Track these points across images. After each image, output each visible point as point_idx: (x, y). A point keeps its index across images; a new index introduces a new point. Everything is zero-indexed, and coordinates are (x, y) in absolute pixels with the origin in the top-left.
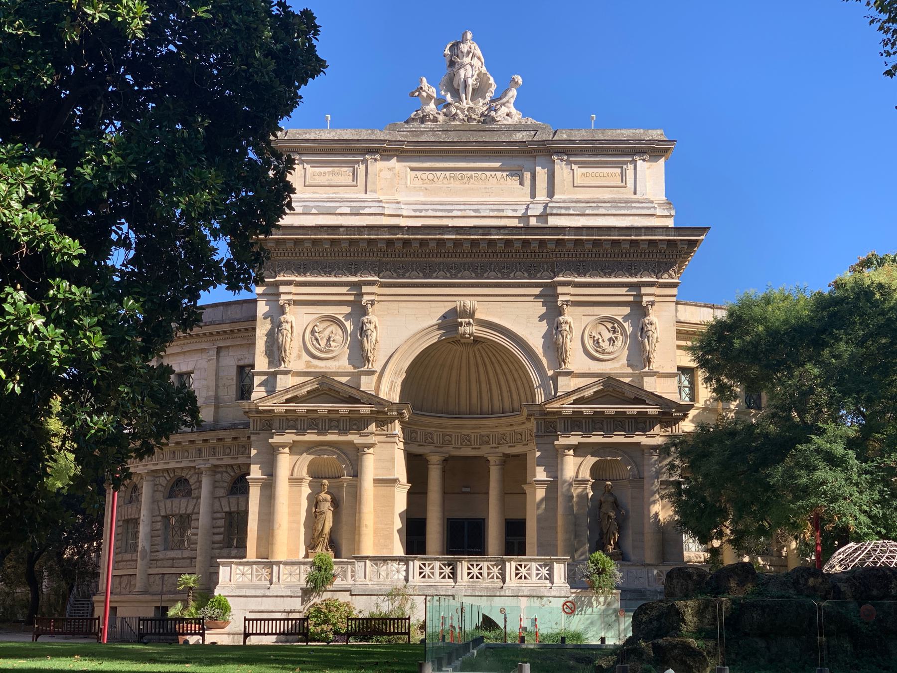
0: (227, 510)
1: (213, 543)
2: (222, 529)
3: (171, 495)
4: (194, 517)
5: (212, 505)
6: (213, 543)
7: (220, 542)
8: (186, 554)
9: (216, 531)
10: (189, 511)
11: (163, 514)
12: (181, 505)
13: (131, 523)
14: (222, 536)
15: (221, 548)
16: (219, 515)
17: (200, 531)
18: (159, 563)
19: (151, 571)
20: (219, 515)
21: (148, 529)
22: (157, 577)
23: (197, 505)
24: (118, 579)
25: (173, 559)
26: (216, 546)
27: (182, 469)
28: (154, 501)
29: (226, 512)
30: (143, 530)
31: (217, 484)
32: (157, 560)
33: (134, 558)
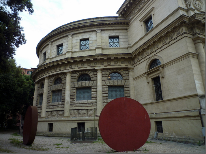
0: (109, 85)
1: (103, 97)
2: (107, 92)
3: (79, 80)
6: (103, 97)
7: (107, 97)
9: (104, 92)
14: (107, 94)
15: (107, 99)
16: (105, 87)
18: (75, 105)
19: (71, 108)
20: (105, 87)
22: (75, 111)
25: (83, 104)
27: (86, 70)
31: (103, 75)
32: (74, 104)
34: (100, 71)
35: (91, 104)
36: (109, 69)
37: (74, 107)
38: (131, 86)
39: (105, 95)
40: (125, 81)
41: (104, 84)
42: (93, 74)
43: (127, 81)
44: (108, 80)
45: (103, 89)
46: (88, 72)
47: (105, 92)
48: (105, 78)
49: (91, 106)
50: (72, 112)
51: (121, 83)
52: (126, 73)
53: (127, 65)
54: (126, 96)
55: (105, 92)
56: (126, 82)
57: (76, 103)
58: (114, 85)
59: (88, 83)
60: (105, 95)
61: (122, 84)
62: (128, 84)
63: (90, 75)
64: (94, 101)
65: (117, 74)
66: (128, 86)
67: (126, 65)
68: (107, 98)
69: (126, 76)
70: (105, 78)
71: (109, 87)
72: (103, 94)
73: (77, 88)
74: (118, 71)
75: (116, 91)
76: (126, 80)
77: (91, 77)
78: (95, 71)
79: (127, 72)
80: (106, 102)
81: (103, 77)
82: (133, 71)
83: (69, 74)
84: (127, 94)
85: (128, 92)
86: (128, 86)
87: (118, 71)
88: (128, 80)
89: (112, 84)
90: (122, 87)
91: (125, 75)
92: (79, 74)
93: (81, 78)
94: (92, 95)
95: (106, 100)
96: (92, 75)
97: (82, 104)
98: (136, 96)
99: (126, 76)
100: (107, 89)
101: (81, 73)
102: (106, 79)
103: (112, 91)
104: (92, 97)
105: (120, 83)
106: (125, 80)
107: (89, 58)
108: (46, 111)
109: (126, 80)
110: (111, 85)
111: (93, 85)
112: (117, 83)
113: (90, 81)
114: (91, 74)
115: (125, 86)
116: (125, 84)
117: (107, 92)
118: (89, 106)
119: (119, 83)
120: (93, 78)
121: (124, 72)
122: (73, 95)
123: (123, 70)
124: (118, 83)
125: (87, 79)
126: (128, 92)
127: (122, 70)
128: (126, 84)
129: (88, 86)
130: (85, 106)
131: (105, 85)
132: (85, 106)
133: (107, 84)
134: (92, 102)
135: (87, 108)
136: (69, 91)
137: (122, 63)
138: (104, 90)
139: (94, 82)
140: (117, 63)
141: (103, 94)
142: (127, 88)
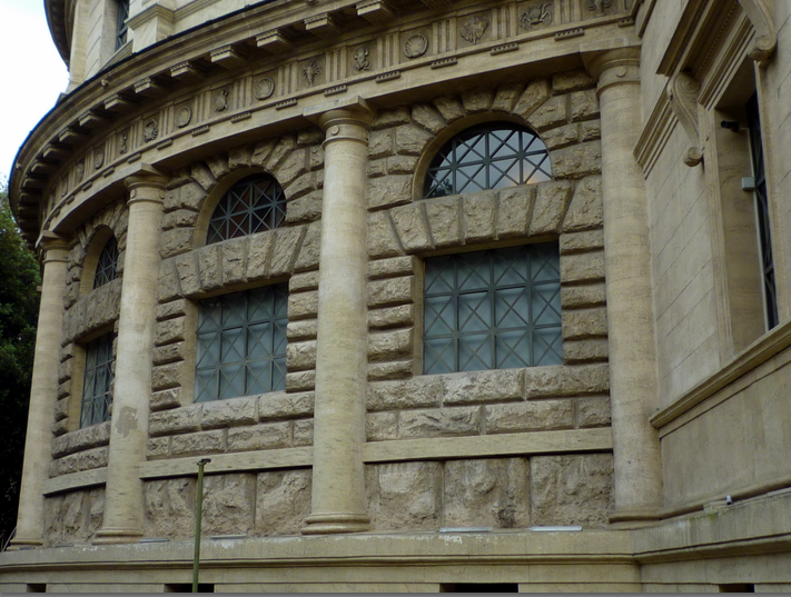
0: (421, 241)
2: (404, 312)
3: (216, 233)
4: (296, 281)
5: (363, 233)
7: (401, 354)
8: (274, 401)
9: (378, 317)
10: (278, 267)
11: (190, 287)
12: (252, 255)
13: (97, 341)
14: (404, 333)
15: (404, 374)
16: (388, 265)
17: (324, 325)
18: (177, 443)
20: (388, 265)
21: (145, 338)
22: (175, 486)
23: (310, 243)
24: (56, 503)
25: (225, 425)
26: (385, 367)
28: (166, 255)
29: (413, 252)
30: (131, 344)
31: (380, 165)
32: (171, 433)
33: (102, 437)
34: (346, 130)
35: (282, 426)
36: (426, 98)
37: (175, 455)
38: (616, 232)
39: (387, 341)
40: (571, 194)
41: (382, 235)
42: (300, 166)
43: (581, 186)
44: (417, 203)
45: (375, 286)
46: (268, 157)
47: (390, 314)
48: (393, 188)
49: (281, 445)
50: (155, 494)
51: (529, 215)
52: (577, 110)
53: (577, 33)
54: (576, 330)
55: (390, 314)
56: (577, 200)
57: (184, 421)
58: (471, 241)
59: (267, 243)
60: (387, 341)
61: (536, 226)
62: (591, 220)
63: (283, 176)
64: (297, 402)
65: (503, 134)
66: (587, 239)
67: (561, 37)
68: (404, 363)
69: (573, 142)
70: (393, 188)
71: (434, 260)
72: (373, 328)
73: (192, 299)
74: (504, 102)
75: (494, 297)
76: (573, 178)
77: (288, 192)
78: (310, 131)
79: (581, 102)
80: (390, 399)
81: (376, 181)
82: (638, 83)
83: (141, 193)
84: (583, 313)
85: (591, 293)
86: (587, 239)
87: (504, 102)
88: (593, 182)
89: (446, 231)
90: (540, 247)
91: (569, 131)
92: (206, 182)
93: (228, 216)
94: (292, 347)
95: (395, 384)
96: (293, 172)
97: (218, 433)
98: (655, 325)
99: (573, 142)
100: (396, 288)
101: (218, 170)
102: (395, 198)
103: (458, 302)
104: (289, 362)
105: (522, 214)
106: (565, 185)
107: (250, 34)
108: (48, 496)
109: (573, 178)
110: (441, 239)
111: (303, 260)
112: (495, 221)
113: (283, 231)
114: (286, 166)
115: (565, 242)
116: (562, 218)
117: (404, 312)
118: (266, 440)
119: (512, 221)
120: (304, 199)
121: (558, 107)
122: (170, 355)
123: (550, 86)
124: (503, 216)
125: (268, 220)
126: (591, 293)
127: (537, 92)
128: (575, 217)
129: (260, 272)
130: (240, 443)
131: (393, 246)
132: (240, 443)
133: (404, 239)
134: (287, 410)
135: (245, 461)
136: (140, 329)
137: (525, 23)
138: (384, 297)
139: (305, 231)
140: (487, 26)
141: (373, 328)
142: (584, 257)
